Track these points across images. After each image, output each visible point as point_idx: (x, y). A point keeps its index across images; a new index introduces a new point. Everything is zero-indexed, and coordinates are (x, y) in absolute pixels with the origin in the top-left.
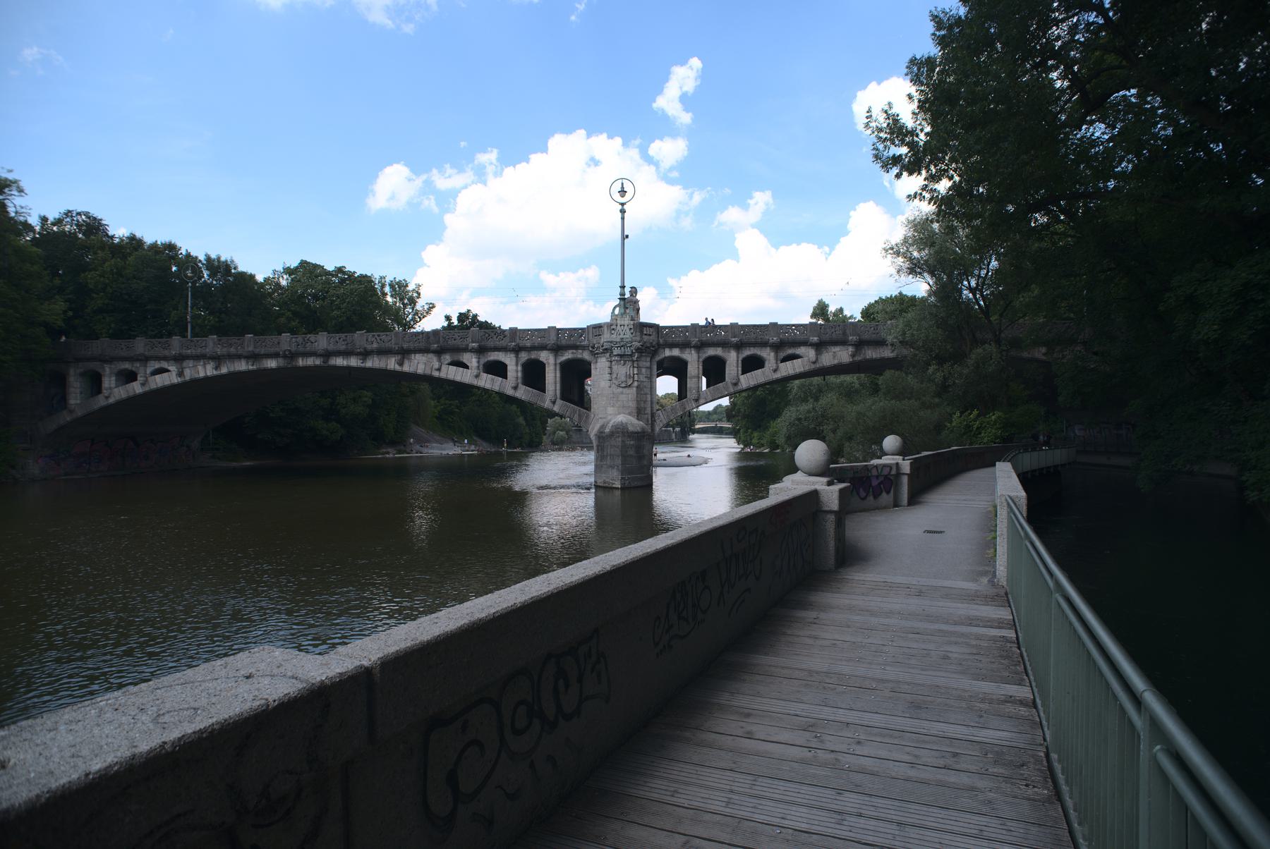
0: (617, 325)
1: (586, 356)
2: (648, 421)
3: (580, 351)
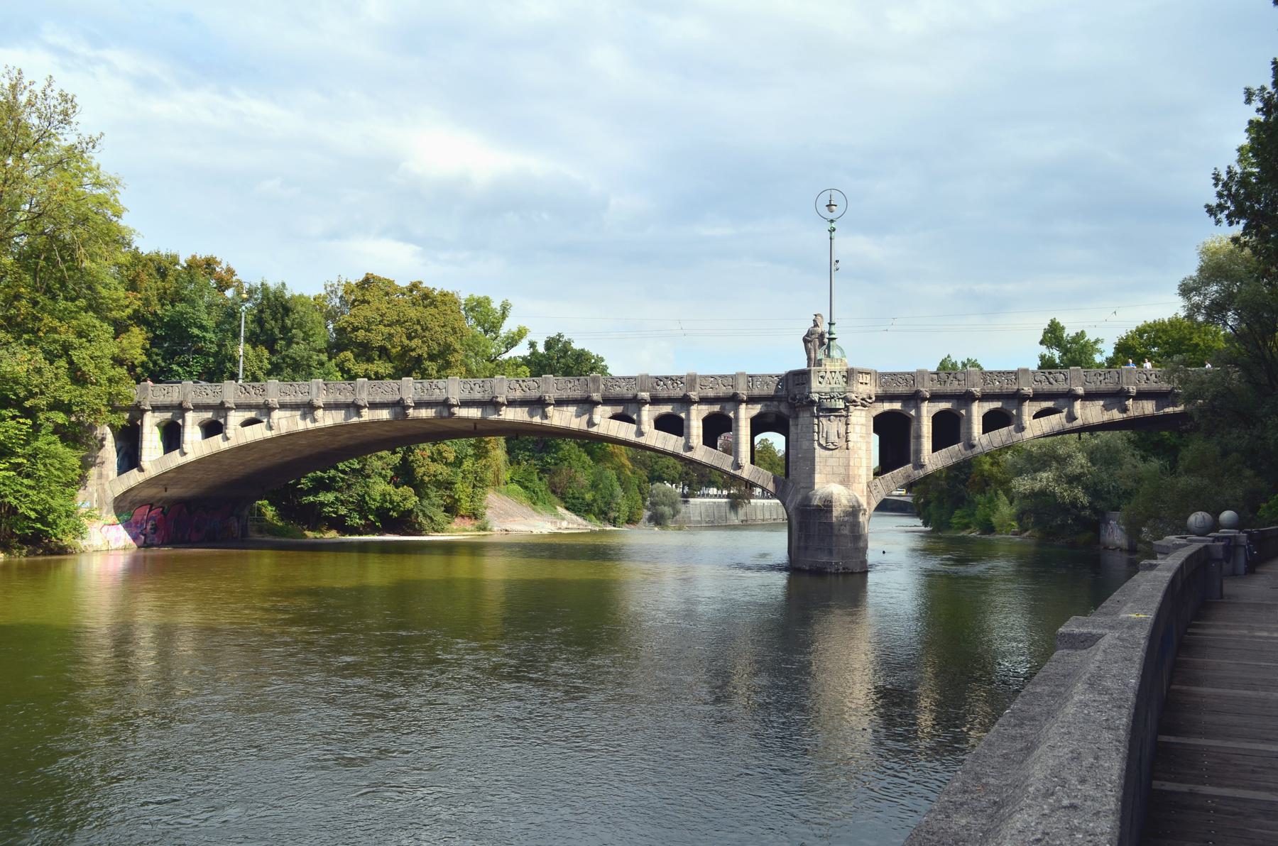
1: (783, 409)
2: (863, 492)
3: (775, 403)
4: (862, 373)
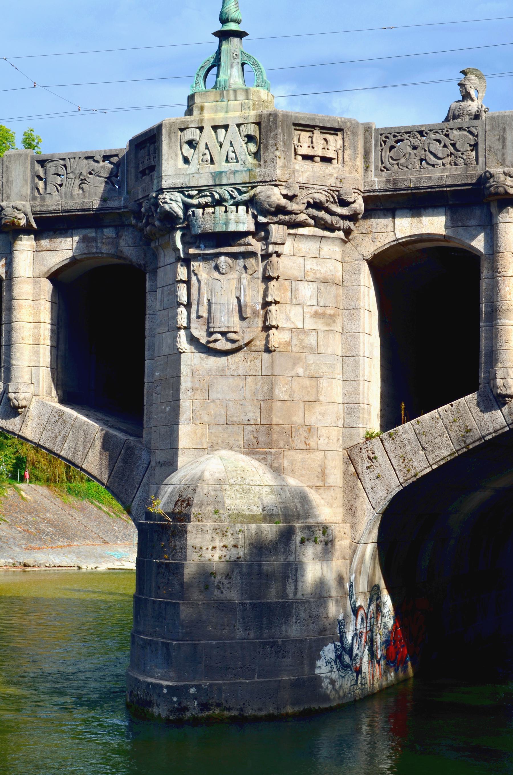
0: (201, 129)
3: (110, 232)
4: (309, 128)
